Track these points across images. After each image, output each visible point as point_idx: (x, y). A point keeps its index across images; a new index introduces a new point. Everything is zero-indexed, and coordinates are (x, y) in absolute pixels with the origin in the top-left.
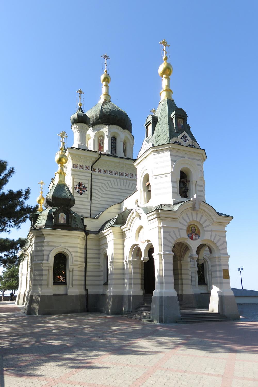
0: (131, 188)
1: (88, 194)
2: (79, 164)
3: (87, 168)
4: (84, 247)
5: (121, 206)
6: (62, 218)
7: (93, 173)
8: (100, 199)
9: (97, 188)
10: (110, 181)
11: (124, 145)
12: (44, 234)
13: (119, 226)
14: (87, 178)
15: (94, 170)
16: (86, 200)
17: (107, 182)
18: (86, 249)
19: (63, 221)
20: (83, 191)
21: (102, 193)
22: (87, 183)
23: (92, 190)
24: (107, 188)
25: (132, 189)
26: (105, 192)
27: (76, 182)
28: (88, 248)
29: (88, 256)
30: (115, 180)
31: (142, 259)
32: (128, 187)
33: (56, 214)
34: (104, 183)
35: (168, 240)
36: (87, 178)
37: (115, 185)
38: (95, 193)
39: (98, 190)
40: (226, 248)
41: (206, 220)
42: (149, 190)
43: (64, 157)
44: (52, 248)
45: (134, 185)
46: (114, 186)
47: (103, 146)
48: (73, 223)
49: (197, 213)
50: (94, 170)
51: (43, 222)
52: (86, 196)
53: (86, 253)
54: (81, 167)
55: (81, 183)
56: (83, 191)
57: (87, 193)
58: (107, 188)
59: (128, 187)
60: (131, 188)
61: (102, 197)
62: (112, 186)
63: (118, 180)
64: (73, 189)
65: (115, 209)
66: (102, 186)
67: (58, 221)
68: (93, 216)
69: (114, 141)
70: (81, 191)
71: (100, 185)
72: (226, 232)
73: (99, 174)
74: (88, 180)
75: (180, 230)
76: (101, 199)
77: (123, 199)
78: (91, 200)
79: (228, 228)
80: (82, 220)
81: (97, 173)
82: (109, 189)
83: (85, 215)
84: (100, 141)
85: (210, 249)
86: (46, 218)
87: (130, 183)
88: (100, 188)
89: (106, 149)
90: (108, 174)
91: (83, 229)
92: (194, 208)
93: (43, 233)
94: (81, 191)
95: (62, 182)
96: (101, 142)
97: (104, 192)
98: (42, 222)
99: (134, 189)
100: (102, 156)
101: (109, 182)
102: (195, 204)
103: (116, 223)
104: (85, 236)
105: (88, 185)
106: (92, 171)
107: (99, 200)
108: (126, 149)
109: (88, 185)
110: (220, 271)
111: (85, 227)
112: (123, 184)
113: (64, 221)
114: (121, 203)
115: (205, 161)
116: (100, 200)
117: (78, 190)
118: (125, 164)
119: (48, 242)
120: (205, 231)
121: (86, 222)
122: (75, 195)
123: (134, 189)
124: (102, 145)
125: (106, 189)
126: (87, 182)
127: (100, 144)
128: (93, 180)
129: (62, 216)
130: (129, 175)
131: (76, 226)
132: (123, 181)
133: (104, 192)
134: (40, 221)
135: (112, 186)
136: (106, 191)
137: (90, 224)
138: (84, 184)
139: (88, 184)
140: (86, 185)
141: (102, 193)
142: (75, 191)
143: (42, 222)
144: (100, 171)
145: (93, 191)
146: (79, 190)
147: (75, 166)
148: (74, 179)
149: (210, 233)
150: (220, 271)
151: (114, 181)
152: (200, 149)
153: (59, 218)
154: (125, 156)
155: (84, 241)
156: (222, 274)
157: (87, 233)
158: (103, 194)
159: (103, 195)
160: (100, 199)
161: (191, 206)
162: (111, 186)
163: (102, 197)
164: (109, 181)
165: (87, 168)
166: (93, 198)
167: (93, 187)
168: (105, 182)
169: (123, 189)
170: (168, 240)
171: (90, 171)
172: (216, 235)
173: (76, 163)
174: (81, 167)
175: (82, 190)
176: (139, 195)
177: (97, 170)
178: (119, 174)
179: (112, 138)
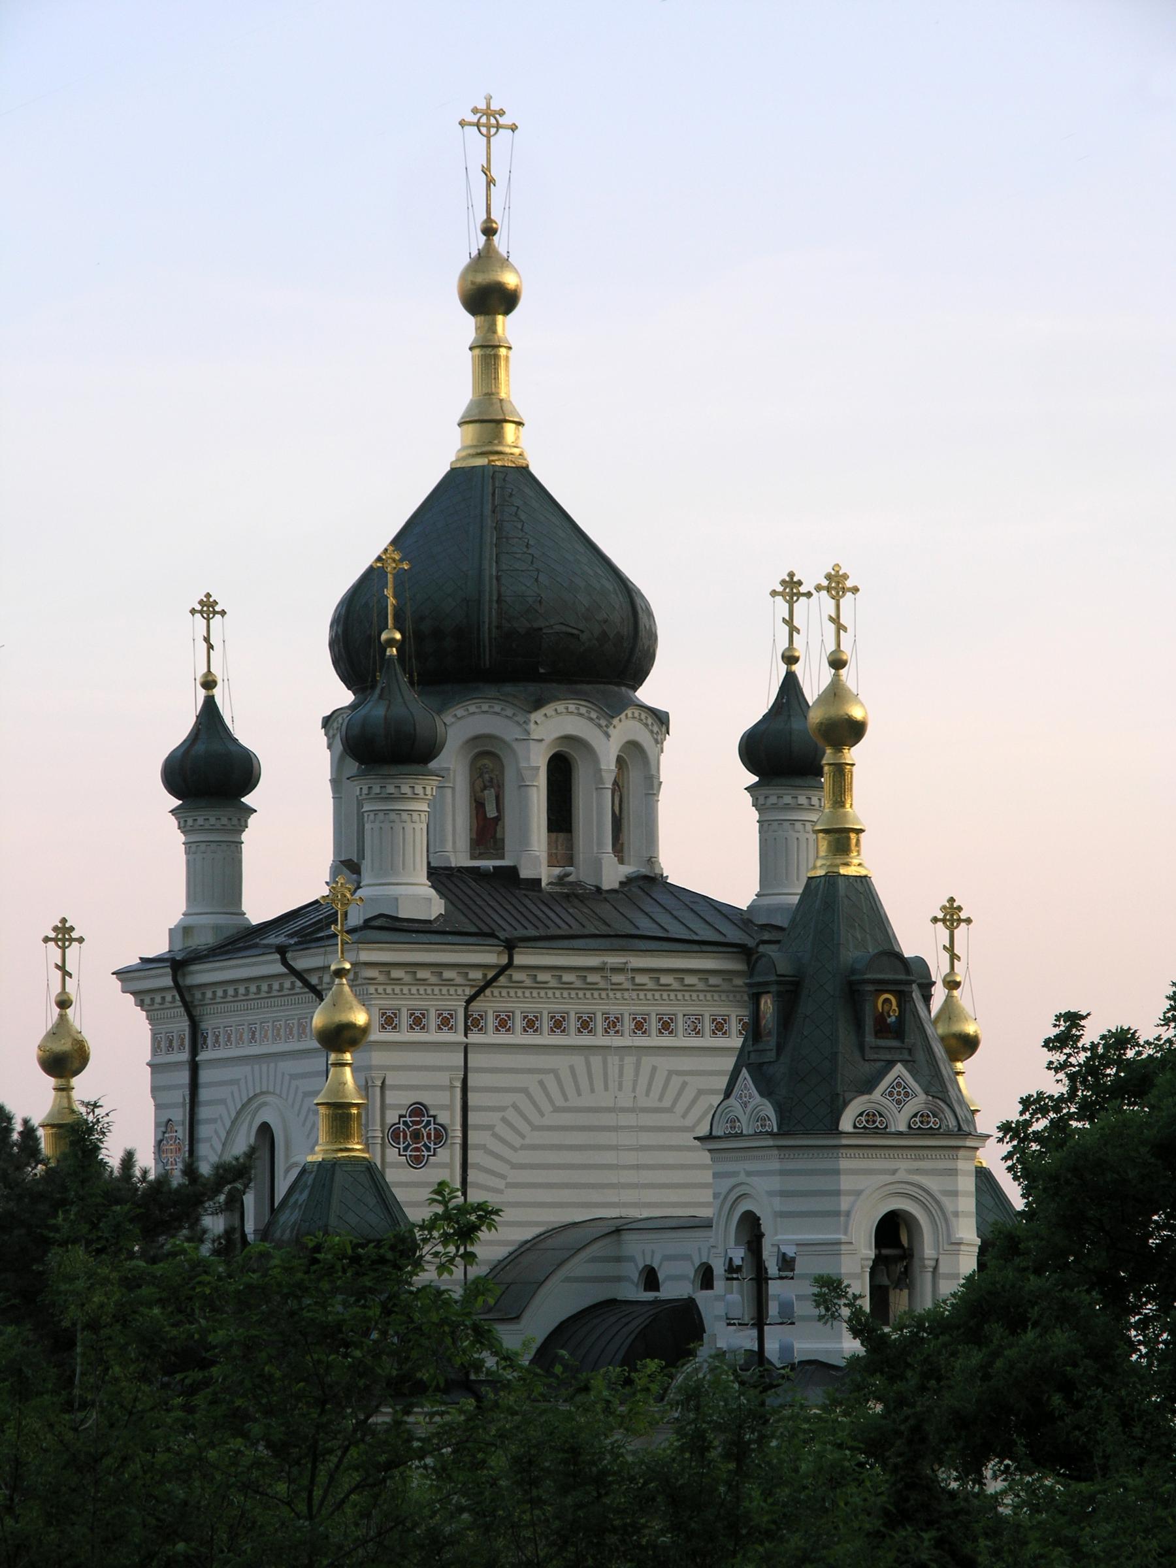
1: (450, 1166)
3: (445, 1022)
8: (503, 1177)
9: (493, 1118)
10: (554, 1072)
14: (443, 1078)
15: (476, 1023)
17: (541, 1083)
20: (428, 1149)
21: (517, 1142)
22: (442, 1107)
24: (542, 1115)
25: (667, 1103)
30: (578, 1060)
34: (525, 1090)
37: (579, 1095)
38: (483, 1147)
39: (497, 1129)
45: (674, 1078)
46: (575, 1101)
47: (498, 819)
50: (476, 1023)
55: (418, 1110)
56: (428, 1149)
58: (542, 1115)
59: (647, 1095)
61: (514, 1166)
62: (566, 1100)
64: (383, 1145)
65: (594, 1260)
66: (515, 1107)
70: (417, 1149)
71: (507, 1099)
76: (509, 1180)
82: (551, 1119)
84: (479, 784)
87: (654, 1069)
88: (504, 1120)
94: (417, 1149)
96: (489, 795)
97: (523, 1137)
105: (450, 1118)
107: (500, 1184)
108: (625, 806)
109: (450, 1118)
117: (405, 1149)
118: (633, 970)
124: (491, 813)
126: (443, 1098)
127: (478, 806)
133: (523, 1137)
135: (566, 1100)
136: (535, 1128)
138: (432, 1113)
139: (450, 1107)
140: (443, 1118)
142: (392, 1154)
144: (503, 1024)
146: (409, 1145)
148: (388, 1093)
151: (572, 1068)
158: (524, 1147)
160: (503, 1177)
162: (560, 1102)
163: (514, 1166)
167: (472, 1118)
168: (530, 1082)
175: (425, 1145)
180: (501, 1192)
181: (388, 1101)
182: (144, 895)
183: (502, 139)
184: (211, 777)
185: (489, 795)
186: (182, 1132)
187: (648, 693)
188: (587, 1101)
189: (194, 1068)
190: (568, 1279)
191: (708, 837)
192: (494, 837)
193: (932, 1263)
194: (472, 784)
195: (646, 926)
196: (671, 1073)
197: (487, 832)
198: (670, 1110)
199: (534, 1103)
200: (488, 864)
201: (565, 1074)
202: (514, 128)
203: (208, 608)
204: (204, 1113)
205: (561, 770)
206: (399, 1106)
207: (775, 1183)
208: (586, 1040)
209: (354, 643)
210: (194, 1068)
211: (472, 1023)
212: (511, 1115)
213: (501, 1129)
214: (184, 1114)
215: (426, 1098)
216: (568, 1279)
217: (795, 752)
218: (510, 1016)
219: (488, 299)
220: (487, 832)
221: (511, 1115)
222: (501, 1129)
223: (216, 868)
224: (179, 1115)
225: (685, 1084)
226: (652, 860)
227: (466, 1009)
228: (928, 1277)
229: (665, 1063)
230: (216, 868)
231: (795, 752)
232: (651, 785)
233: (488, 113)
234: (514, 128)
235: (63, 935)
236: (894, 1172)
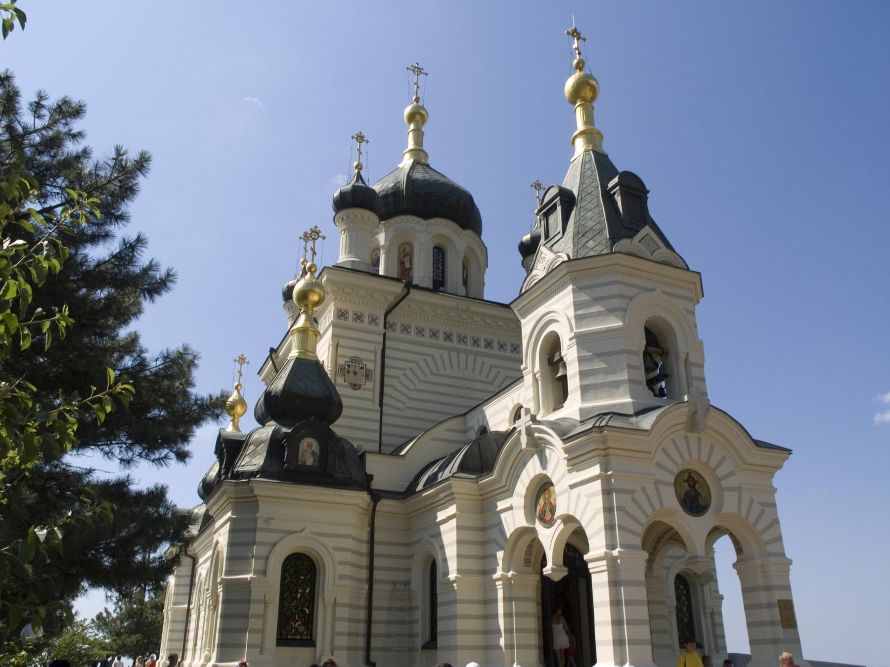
0: (487, 377)
1: (373, 390)
2: (351, 309)
3: (374, 320)
4: (365, 536)
5: (465, 422)
6: (308, 450)
7: (389, 334)
8: (404, 403)
11: (465, 268)
12: (256, 496)
13: (473, 477)
14: (371, 347)
15: (391, 326)
16: (369, 405)
17: (425, 360)
18: (371, 542)
19: (310, 461)
21: (412, 387)
23: (386, 379)
25: (490, 379)
27: (341, 356)
28: (376, 539)
29: (377, 562)
30: (445, 353)
31: (547, 570)
32: (480, 374)
33: (293, 440)
34: (416, 363)
35: (627, 513)
36: (371, 347)
38: (393, 386)
40: (779, 539)
41: (723, 459)
42: (559, 375)
43: (317, 290)
44: (281, 535)
47: (410, 269)
48: (339, 468)
49: (699, 439)
50: (391, 326)
51: (254, 461)
52: (369, 395)
53: (371, 555)
54: (358, 317)
57: (373, 386)
59: (480, 374)
60: (487, 377)
61: (409, 398)
62: (438, 370)
63: (454, 355)
65: (449, 430)
66: (411, 369)
67: (298, 460)
68: (384, 450)
69: (439, 254)
72: (774, 491)
73: (404, 336)
74: (375, 352)
75: (660, 486)
77: (468, 407)
78: (381, 405)
79: (778, 479)
80: (362, 457)
81: (398, 334)
83: (366, 446)
84: (402, 255)
85: (736, 543)
86: (264, 448)
87: (483, 363)
88: (404, 374)
89: (422, 272)
91: (364, 483)
92: (693, 424)
93: (256, 492)
95: (310, 354)
96: (407, 259)
97: (415, 385)
98: (252, 461)
99: (494, 380)
100: (412, 290)
101: (429, 359)
102: (695, 413)
103: (462, 468)
104: (369, 505)
105: (374, 366)
106: (385, 327)
110: (770, 606)
111: (370, 478)
112: (466, 366)
113: (315, 461)
114: (469, 416)
115: (698, 302)
116: (406, 408)
119: (268, 520)
120: (723, 489)
121: (375, 465)
122: (340, 390)
123: (494, 380)
124: (407, 266)
125: (422, 377)
126: (371, 356)
127: (402, 263)
128: (387, 352)
129: (310, 446)
130: (482, 343)
131: (348, 476)
132: (467, 358)
133: (415, 385)
134: (247, 459)
135: (438, 370)
136: (421, 381)
137: (383, 471)
139: (375, 361)
140: (370, 366)
141: (412, 387)
143: (252, 461)
144: (406, 329)
145: (386, 380)
147: (341, 314)
149: (736, 494)
150: (770, 606)
151: (441, 355)
152: (688, 269)
153: (300, 452)
154: (467, 293)
155: (366, 520)
156: (776, 614)
157: (376, 496)
158: (415, 390)
160: (404, 403)
161: (684, 419)
162: (435, 371)
163: (409, 398)
164: (428, 355)
165: (374, 320)
166: (385, 400)
167: (387, 371)
169: (467, 379)
170: (627, 513)
171: (381, 328)
172: (752, 501)
173: (344, 307)
174: (358, 317)
176: (525, 393)
177: (399, 327)
178: (455, 337)
179: (434, 248)
180: (402, 410)
181: (339, 353)
185: (407, 259)
190: (434, 439)
192: (408, 275)
193: (685, 356)
194: (399, 255)
196: (492, 366)
198: (492, 383)
199: (422, 370)
201: (438, 360)
202: (426, 74)
206: (345, 357)
208: (447, 344)
212: (408, 373)
213: (403, 379)
215: (361, 355)
216: (434, 439)
218: (409, 327)
221: (408, 373)
222: (403, 379)
225: (499, 373)
227: (387, 314)
228: (682, 365)
229: (489, 361)
233: (418, 68)
234: (426, 74)
236: (653, 290)
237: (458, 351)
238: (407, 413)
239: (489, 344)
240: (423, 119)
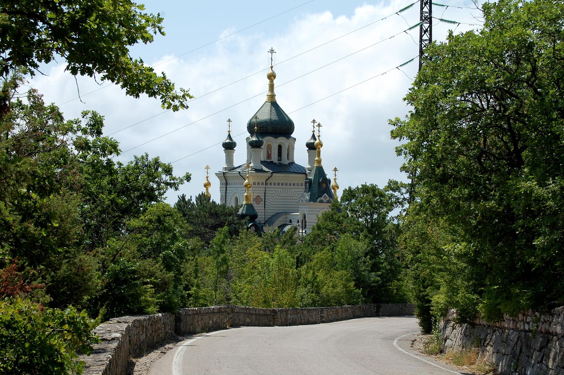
3: (262, 184)
14: (262, 192)
16: (261, 208)
26: (275, 200)
36: (262, 192)
55: (258, 196)
57: (263, 203)
90: (277, 186)
105: (263, 197)
130: (292, 185)
144: (271, 184)
159: (273, 203)
165: (262, 184)
173: (255, 181)
174: (258, 184)
182: (221, 165)
183: (274, 54)
184: (229, 146)
186: (224, 197)
187: (293, 135)
188: (282, 195)
189: (226, 188)
191: (301, 157)
195: (292, 170)
197: (269, 156)
200: (269, 161)
203: (229, 121)
204: (227, 194)
205: (280, 147)
207: (308, 209)
208: (282, 187)
209: (251, 128)
210: (226, 188)
211: (266, 184)
214: (224, 197)
215: (259, 195)
217: (313, 147)
219: (271, 77)
220: (269, 156)
223: (229, 159)
224: (224, 194)
226: (293, 160)
229: (294, 190)
230: (229, 159)
231: (313, 147)
232: (293, 148)
235: (207, 168)
237: (285, 188)
238: (271, 208)
239: (294, 185)
240: (275, 77)
